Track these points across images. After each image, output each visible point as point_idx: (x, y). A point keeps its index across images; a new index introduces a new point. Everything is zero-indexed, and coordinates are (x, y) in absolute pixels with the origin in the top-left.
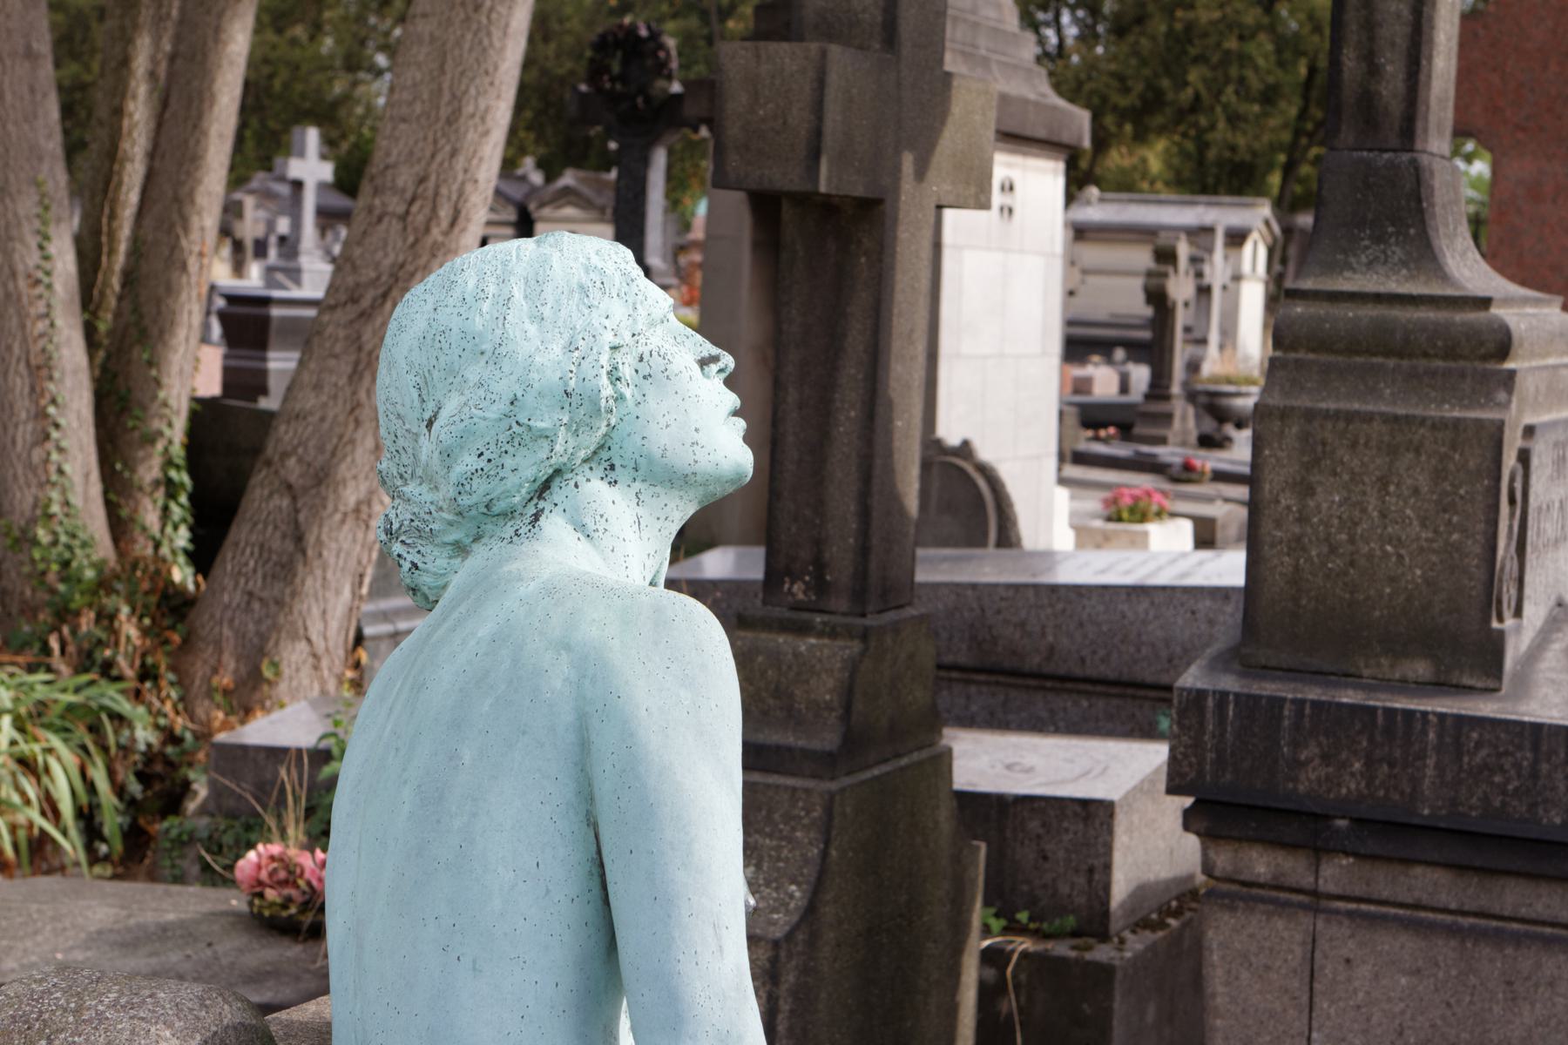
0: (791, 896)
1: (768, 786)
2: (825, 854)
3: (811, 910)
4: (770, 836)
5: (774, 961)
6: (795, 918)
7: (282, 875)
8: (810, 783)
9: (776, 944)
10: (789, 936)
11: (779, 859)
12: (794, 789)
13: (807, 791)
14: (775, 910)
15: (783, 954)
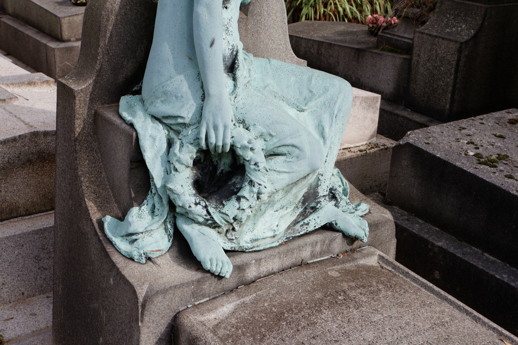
0: (471, 33)
1: (472, 5)
2: (482, 23)
3: (475, 36)
4: (471, 18)
5: (460, 47)
6: (470, 38)
7: (375, 21)
8: (482, 5)
9: (461, 43)
10: (467, 42)
11: (471, 24)
12: (478, 6)
13: (481, 7)
14: (466, 36)
15: (463, 46)
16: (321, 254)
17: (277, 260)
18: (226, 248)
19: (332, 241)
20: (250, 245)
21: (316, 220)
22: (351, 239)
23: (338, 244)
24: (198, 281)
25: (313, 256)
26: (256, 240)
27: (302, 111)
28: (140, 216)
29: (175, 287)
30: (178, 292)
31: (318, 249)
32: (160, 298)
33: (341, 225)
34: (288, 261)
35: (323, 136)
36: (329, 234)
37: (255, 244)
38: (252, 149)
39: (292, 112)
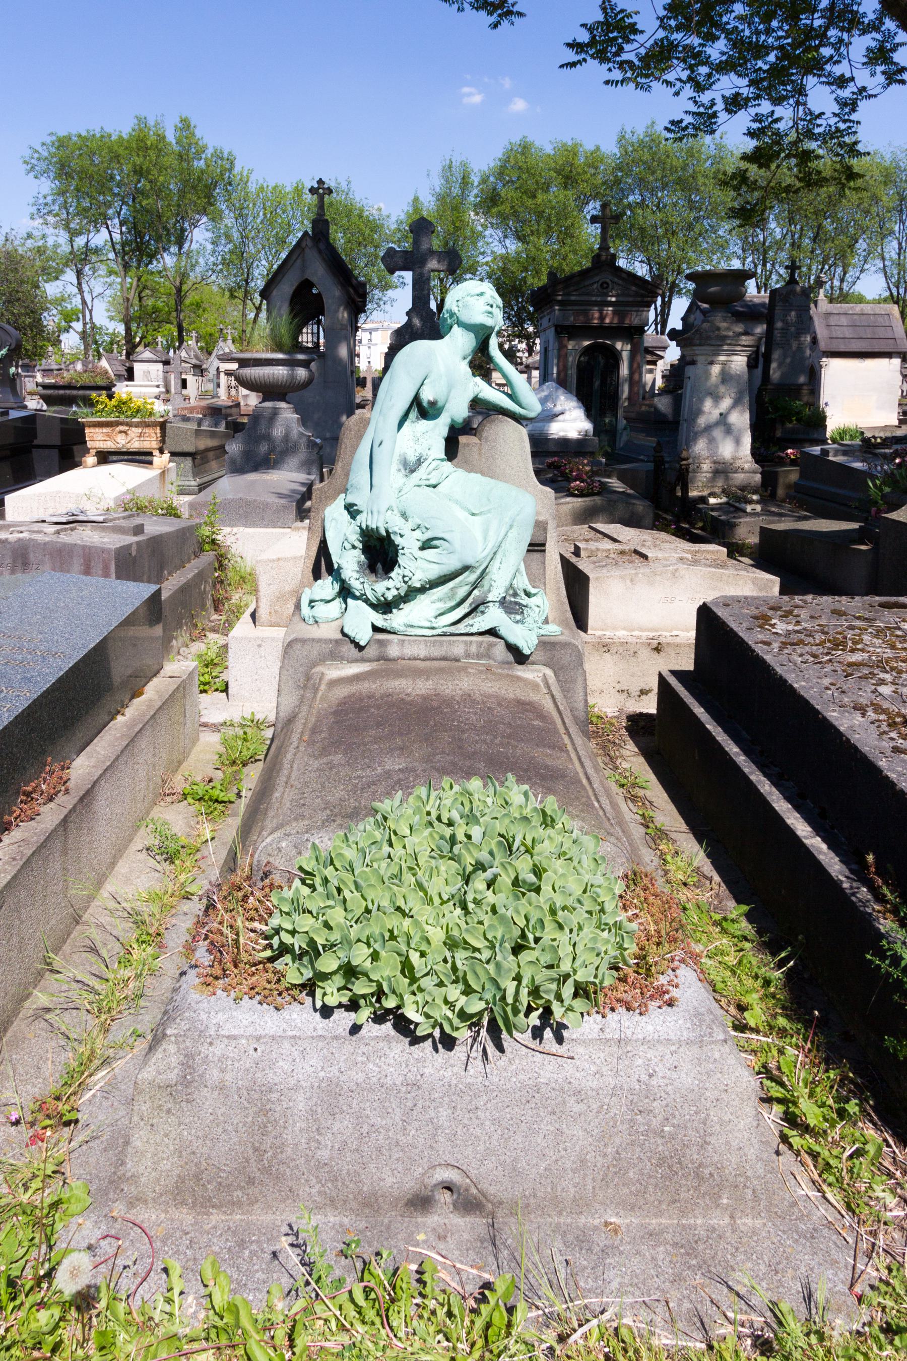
16: (479, 656)
17: (422, 646)
18: (376, 624)
19: (491, 645)
20: (402, 628)
21: (480, 623)
22: (513, 649)
23: (500, 650)
24: (337, 641)
25: (468, 656)
26: (412, 626)
27: (473, 514)
28: (322, 588)
29: (313, 640)
30: (316, 646)
31: (474, 649)
32: (299, 645)
33: (503, 632)
34: (437, 652)
35: (485, 539)
36: (489, 639)
37: (409, 629)
38: (401, 536)
39: (463, 515)
